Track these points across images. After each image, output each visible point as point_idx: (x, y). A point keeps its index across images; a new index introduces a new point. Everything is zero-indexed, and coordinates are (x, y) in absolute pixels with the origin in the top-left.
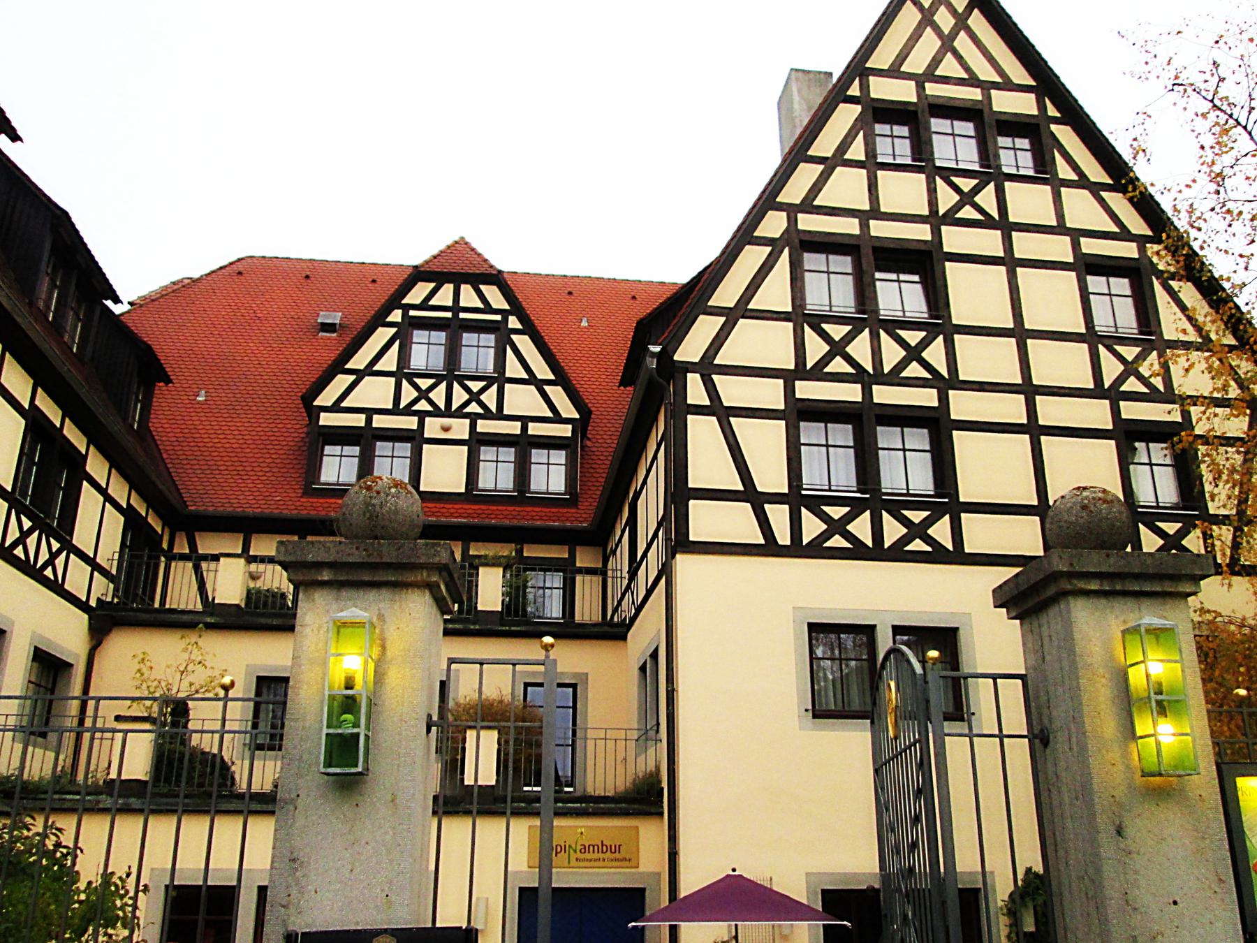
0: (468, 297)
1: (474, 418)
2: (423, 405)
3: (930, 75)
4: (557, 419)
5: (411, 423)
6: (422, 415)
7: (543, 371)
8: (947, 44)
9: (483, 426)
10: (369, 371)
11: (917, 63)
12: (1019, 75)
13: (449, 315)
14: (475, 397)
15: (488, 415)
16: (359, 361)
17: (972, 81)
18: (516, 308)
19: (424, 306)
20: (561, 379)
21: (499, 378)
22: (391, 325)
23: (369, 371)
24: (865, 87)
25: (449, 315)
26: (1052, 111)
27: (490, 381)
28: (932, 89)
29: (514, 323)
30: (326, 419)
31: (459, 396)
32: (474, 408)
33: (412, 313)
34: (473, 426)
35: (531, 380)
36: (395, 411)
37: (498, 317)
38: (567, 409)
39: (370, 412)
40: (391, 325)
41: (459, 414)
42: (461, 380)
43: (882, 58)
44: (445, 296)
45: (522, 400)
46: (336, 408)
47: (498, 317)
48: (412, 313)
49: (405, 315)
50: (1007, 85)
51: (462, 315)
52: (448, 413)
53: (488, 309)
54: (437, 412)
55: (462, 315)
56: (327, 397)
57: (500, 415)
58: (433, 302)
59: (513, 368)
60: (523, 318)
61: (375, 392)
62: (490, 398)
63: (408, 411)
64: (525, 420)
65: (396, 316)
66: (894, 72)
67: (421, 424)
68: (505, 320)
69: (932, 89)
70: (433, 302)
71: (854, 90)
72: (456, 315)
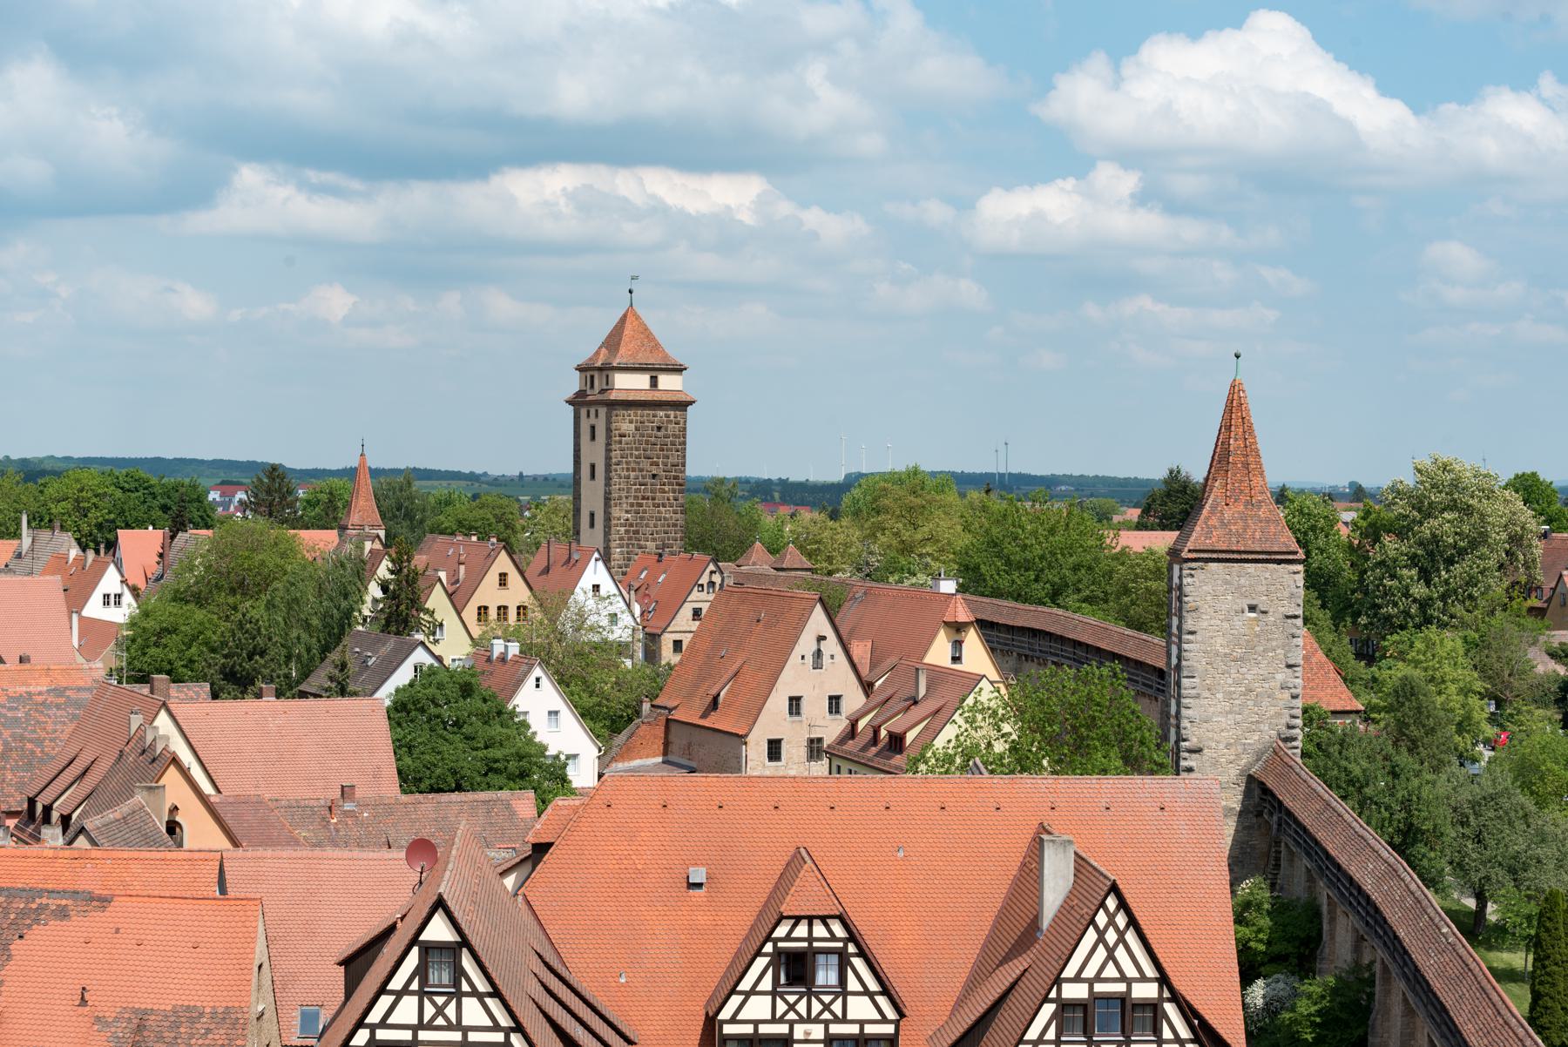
0: (819, 930)
1: (827, 1023)
2: (792, 1016)
3: (1098, 978)
4: (884, 1020)
5: (783, 1029)
6: (792, 1023)
7: (873, 986)
8: (1111, 956)
9: (835, 1029)
10: (753, 991)
11: (1089, 972)
12: (1150, 972)
13: (805, 944)
14: (827, 1007)
15: (836, 1020)
16: (745, 985)
17: (1123, 978)
18: (852, 937)
19: (788, 938)
20: (885, 992)
21: (843, 992)
22: (766, 955)
23: (753, 991)
24: (1059, 991)
25: (805, 944)
26: (1166, 994)
27: (837, 995)
28: (1099, 988)
29: (852, 949)
30: (728, 1029)
31: (816, 1007)
32: (826, 1016)
33: (780, 944)
34: (827, 1029)
35: (866, 992)
36: (774, 1020)
37: (840, 945)
38: (891, 1014)
39: (756, 1023)
40: (766, 955)
41: (817, 1021)
42: (817, 995)
43: (1069, 972)
44: (801, 931)
45: (860, 1008)
46: (733, 1020)
47: (840, 945)
48: (780, 944)
49: (775, 946)
50: (1143, 979)
51: (816, 944)
52: (809, 1020)
53: (833, 938)
54: (802, 1020)
55: (816, 944)
56: (725, 1014)
57: (844, 1020)
58: (794, 935)
59: (853, 984)
60: (858, 945)
61: (759, 1008)
62: (837, 1007)
63: (781, 1020)
64: (862, 1023)
65: (768, 948)
66: (1077, 979)
67: (791, 1029)
68: (846, 946)
69: (1099, 988)
70: (794, 935)
71: (1053, 994)
72: (810, 944)
